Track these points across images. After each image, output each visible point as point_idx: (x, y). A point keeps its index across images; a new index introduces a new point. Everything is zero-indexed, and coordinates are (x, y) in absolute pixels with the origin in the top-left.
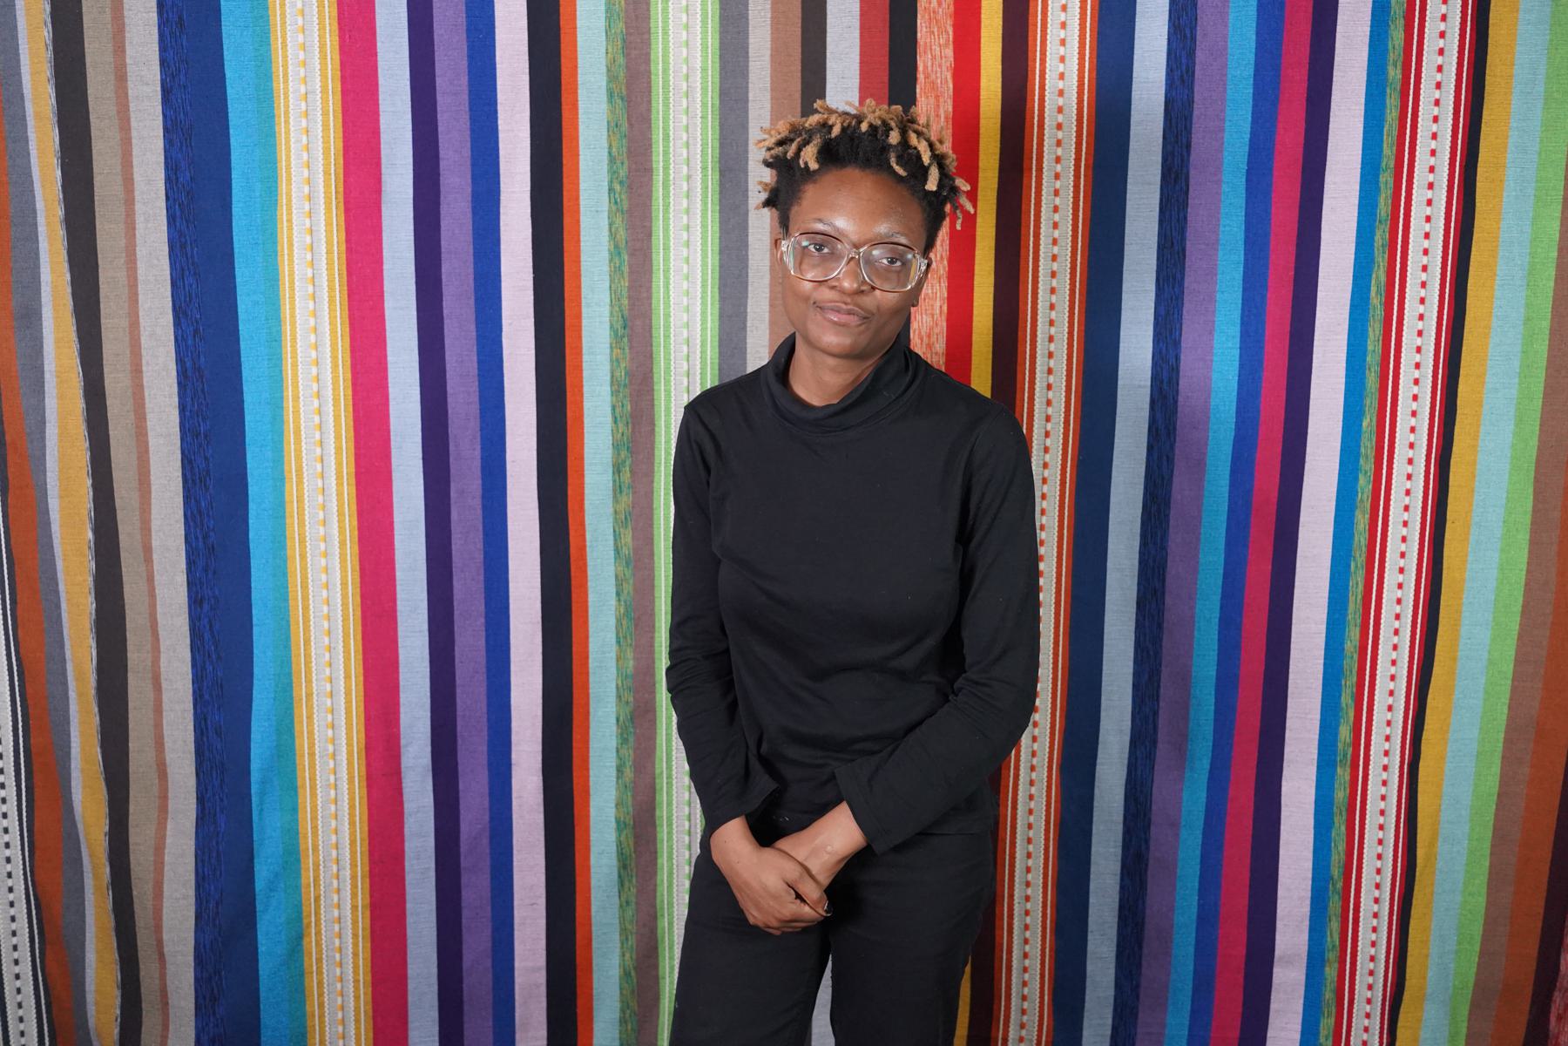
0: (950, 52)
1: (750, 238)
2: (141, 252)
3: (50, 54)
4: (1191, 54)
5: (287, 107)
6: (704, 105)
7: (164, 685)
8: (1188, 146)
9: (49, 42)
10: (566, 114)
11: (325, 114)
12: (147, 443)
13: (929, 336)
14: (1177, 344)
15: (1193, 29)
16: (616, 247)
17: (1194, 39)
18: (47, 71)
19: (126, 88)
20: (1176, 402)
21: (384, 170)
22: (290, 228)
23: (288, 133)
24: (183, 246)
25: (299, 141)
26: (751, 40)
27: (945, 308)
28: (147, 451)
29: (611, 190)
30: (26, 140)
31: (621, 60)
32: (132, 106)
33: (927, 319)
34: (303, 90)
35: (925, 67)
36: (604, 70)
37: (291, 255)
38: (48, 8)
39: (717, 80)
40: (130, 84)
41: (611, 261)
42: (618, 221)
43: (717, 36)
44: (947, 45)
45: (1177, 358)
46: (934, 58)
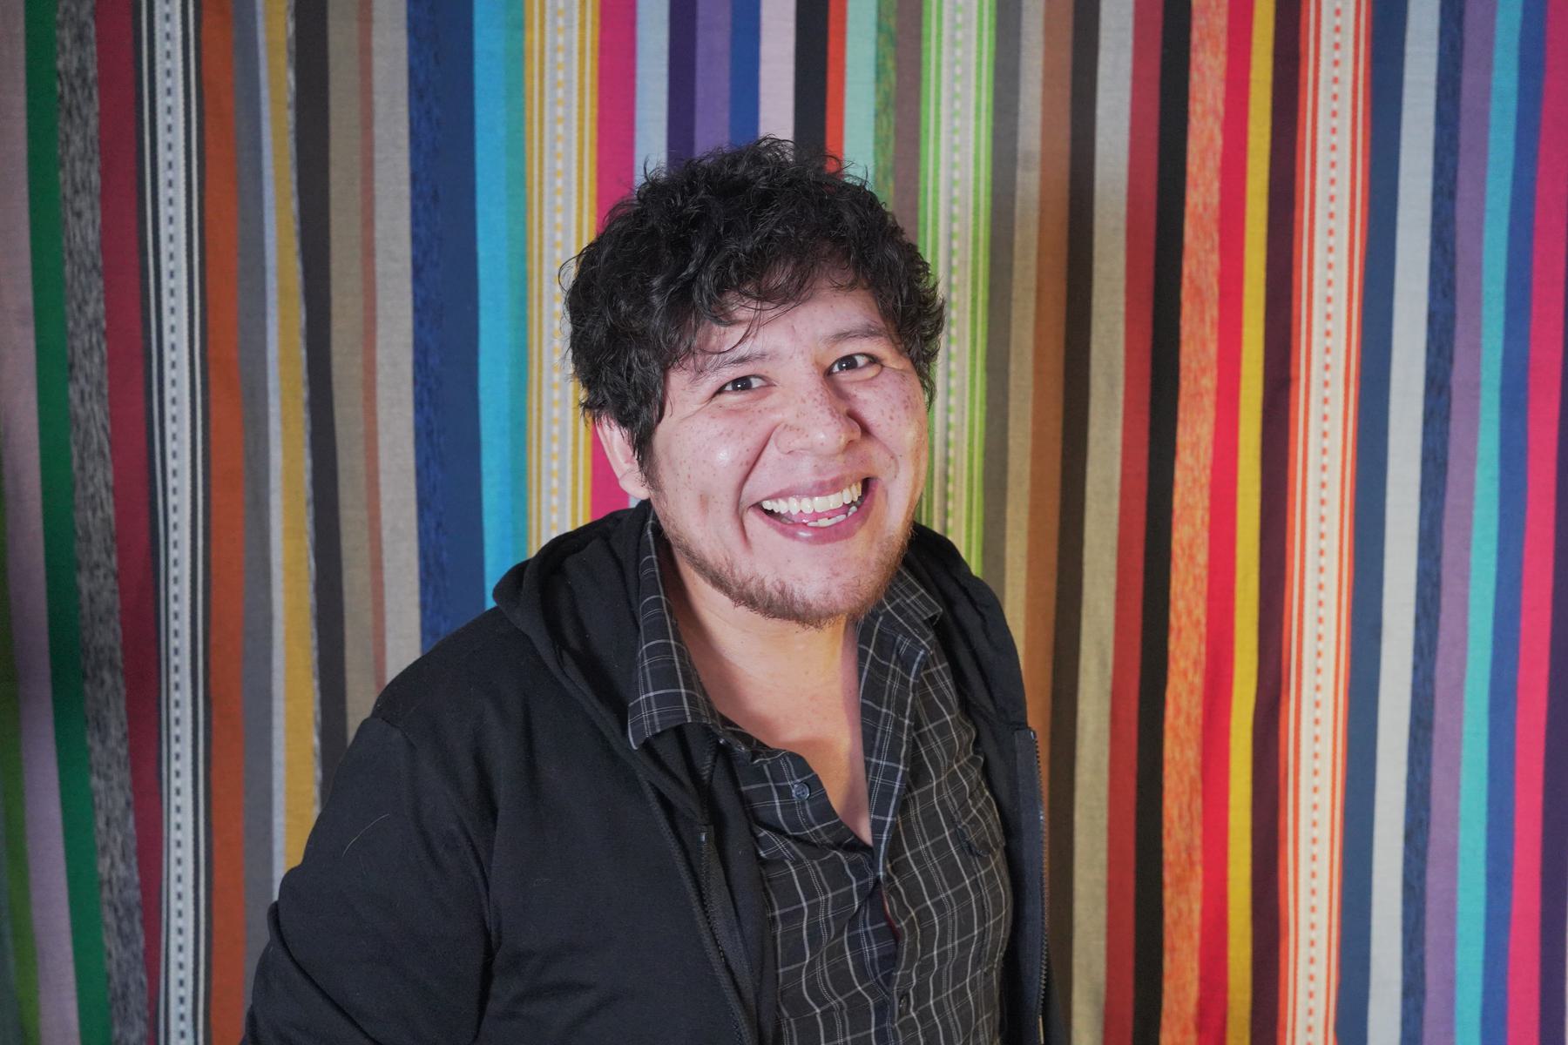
1: (1011, 442)
2: (384, 440)
4: (1452, 268)
5: (540, 289)
8: (1451, 360)
13: (1191, 546)
14: (1438, 559)
15: (1453, 244)
17: (1454, 254)
18: (294, 245)
19: (373, 265)
20: (1437, 619)
23: (540, 316)
24: (429, 434)
26: (1017, 237)
27: (1207, 518)
30: (264, 315)
32: (380, 282)
37: (539, 447)
38: (294, 177)
45: (1439, 575)
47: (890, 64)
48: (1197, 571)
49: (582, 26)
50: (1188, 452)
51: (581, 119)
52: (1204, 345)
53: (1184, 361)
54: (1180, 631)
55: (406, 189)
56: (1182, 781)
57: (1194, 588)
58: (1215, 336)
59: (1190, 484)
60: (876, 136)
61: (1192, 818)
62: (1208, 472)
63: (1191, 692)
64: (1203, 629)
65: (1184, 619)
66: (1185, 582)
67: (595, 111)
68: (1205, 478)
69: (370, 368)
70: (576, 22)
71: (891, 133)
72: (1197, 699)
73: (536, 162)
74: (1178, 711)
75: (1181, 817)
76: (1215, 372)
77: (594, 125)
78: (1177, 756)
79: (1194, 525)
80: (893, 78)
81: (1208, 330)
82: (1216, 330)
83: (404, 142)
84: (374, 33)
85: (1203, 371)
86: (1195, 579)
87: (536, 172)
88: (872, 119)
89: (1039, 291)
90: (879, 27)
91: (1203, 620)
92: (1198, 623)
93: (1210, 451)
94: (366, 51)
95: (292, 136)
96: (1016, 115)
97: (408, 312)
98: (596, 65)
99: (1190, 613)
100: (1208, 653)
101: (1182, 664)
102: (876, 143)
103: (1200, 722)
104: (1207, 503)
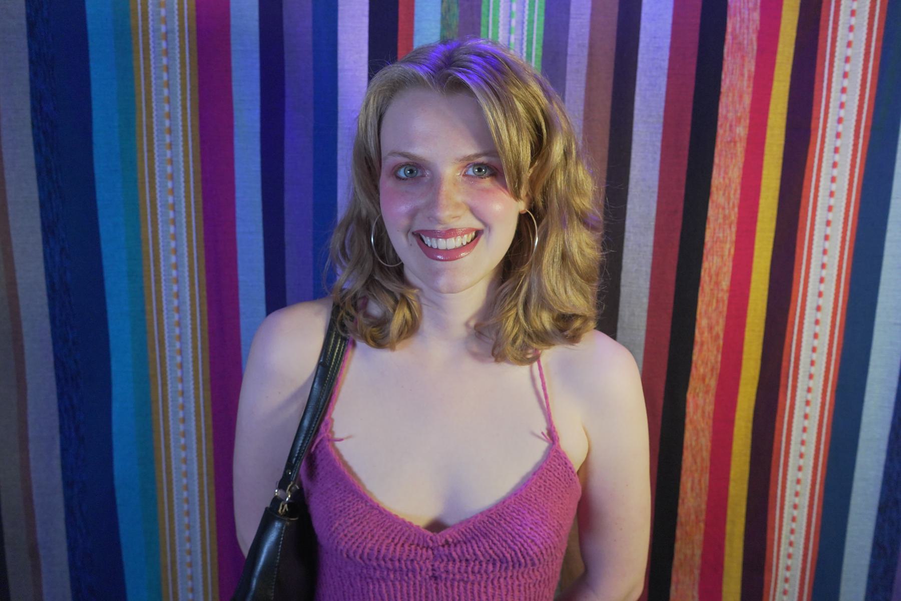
0: (756, 16)
11: (182, 52)
12: (22, 346)
13: (717, 275)
21: (235, 106)
22: (151, 158)
25: (159, 77)
28: (23, 354)
31: (456, 10)
33: (716, 260)
34: (163, 28)
35: (734, 29)
36: (439, 17)
39: (541, 32)
44: (754, 9)
46: (742, 20)
48: (720, 295)
50: (721, 193)
52: (741, 97)
53: (722, 111)
54: (702, 344)
56: (696, 463)
57: (717, 308)
58: (750, 90)
59: (721, 220)
61: (701, 489)
62: (736, 210)
63: (707, 392)
64: (721, 342)
65: (706, 334)
66: (709, 304)
68: (734, 217)
72: (711, 398)
74: (696, 406)
75: (692, 489)
76: (748, 121)
78: (694, 443)
79: (722, 256)
81: (745, 83)
82: (751, 85)
85: (739, 120)
86: (718, 301)
89: (591, 46)
91: (722, 336)
92: (717, 336)
93: (739, 192)
99: (711, 328)
100: (722, 362)
101: (702, 370)
103: (712, 415)
104: (734, 238)
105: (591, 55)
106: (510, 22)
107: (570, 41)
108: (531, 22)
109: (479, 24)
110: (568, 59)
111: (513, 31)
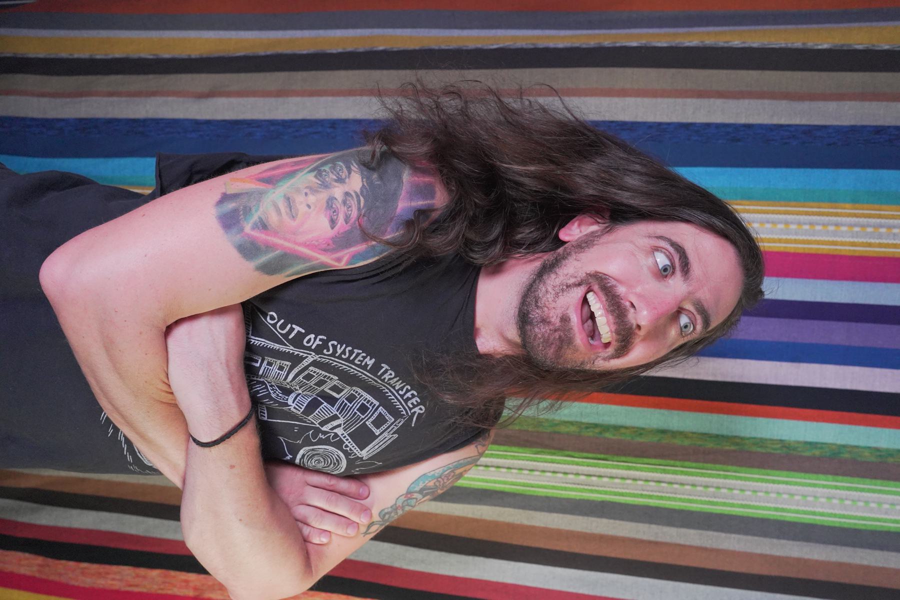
1: (555, 515)
3: (721, 44)
6: (650, 497)
7: (280, 100)
9: (730, 44)
10: (651, 399)
16: (557, 425)
29: (596, 426)
31: (687, 443)
36: (681, 429)
38: (755, 45)
39: (667, 506)
40: (694, 100)
41: (547, 420)
42: (572, 429)
43: (698, 510)
47: (817, 453)
49: (853, 244)
51: (787, 241)
55: (743, 120)
60: (766, 440)
67: (792, 251)
69: (623, 93)
70: (856, 240)
71: (769, 450)
73: (759, 208)
77: (782, 250)
80: (807, 454)
83: (775, 121)
84: (853, 103)
87: (752, 207)
88: (779, 438)
90: (844, 446)
94: (840, 97)
95: (783, 45)
96: (778, 538)
97: (659, 119)
98: (825, 252)
102: (761, 439)
105: (650, 542)
106: (677, 483)
107: (660, 527)
108: (674, 499)
109: (676, 460)
110: (647, 525)
111: (670, 486)
